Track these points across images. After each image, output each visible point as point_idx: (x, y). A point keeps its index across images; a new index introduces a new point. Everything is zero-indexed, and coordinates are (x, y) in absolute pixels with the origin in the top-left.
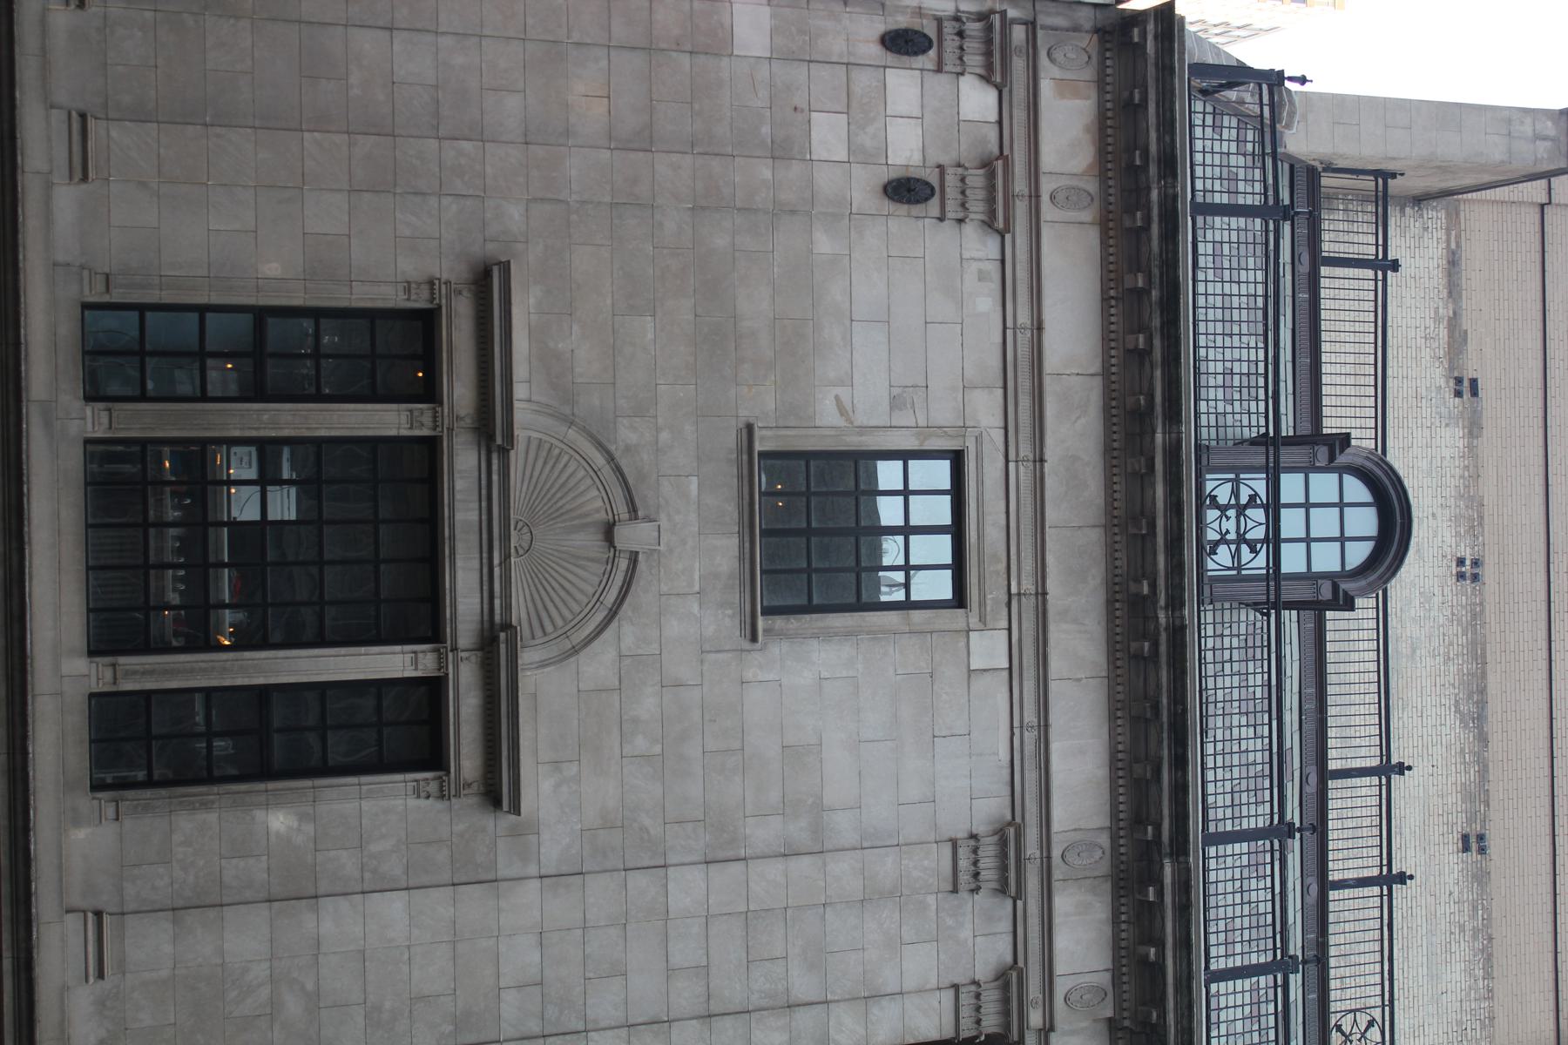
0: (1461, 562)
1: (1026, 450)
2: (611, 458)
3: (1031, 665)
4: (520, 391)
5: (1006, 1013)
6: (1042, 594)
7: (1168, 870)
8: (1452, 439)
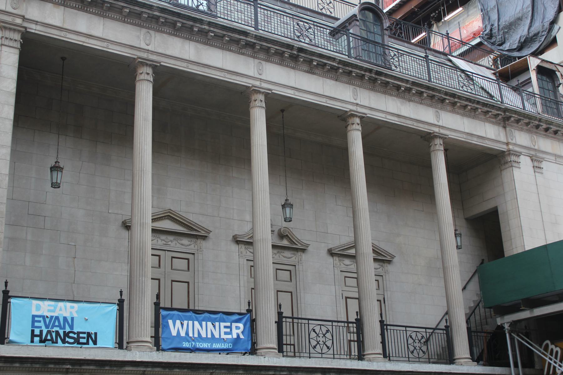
5: (14, 30)
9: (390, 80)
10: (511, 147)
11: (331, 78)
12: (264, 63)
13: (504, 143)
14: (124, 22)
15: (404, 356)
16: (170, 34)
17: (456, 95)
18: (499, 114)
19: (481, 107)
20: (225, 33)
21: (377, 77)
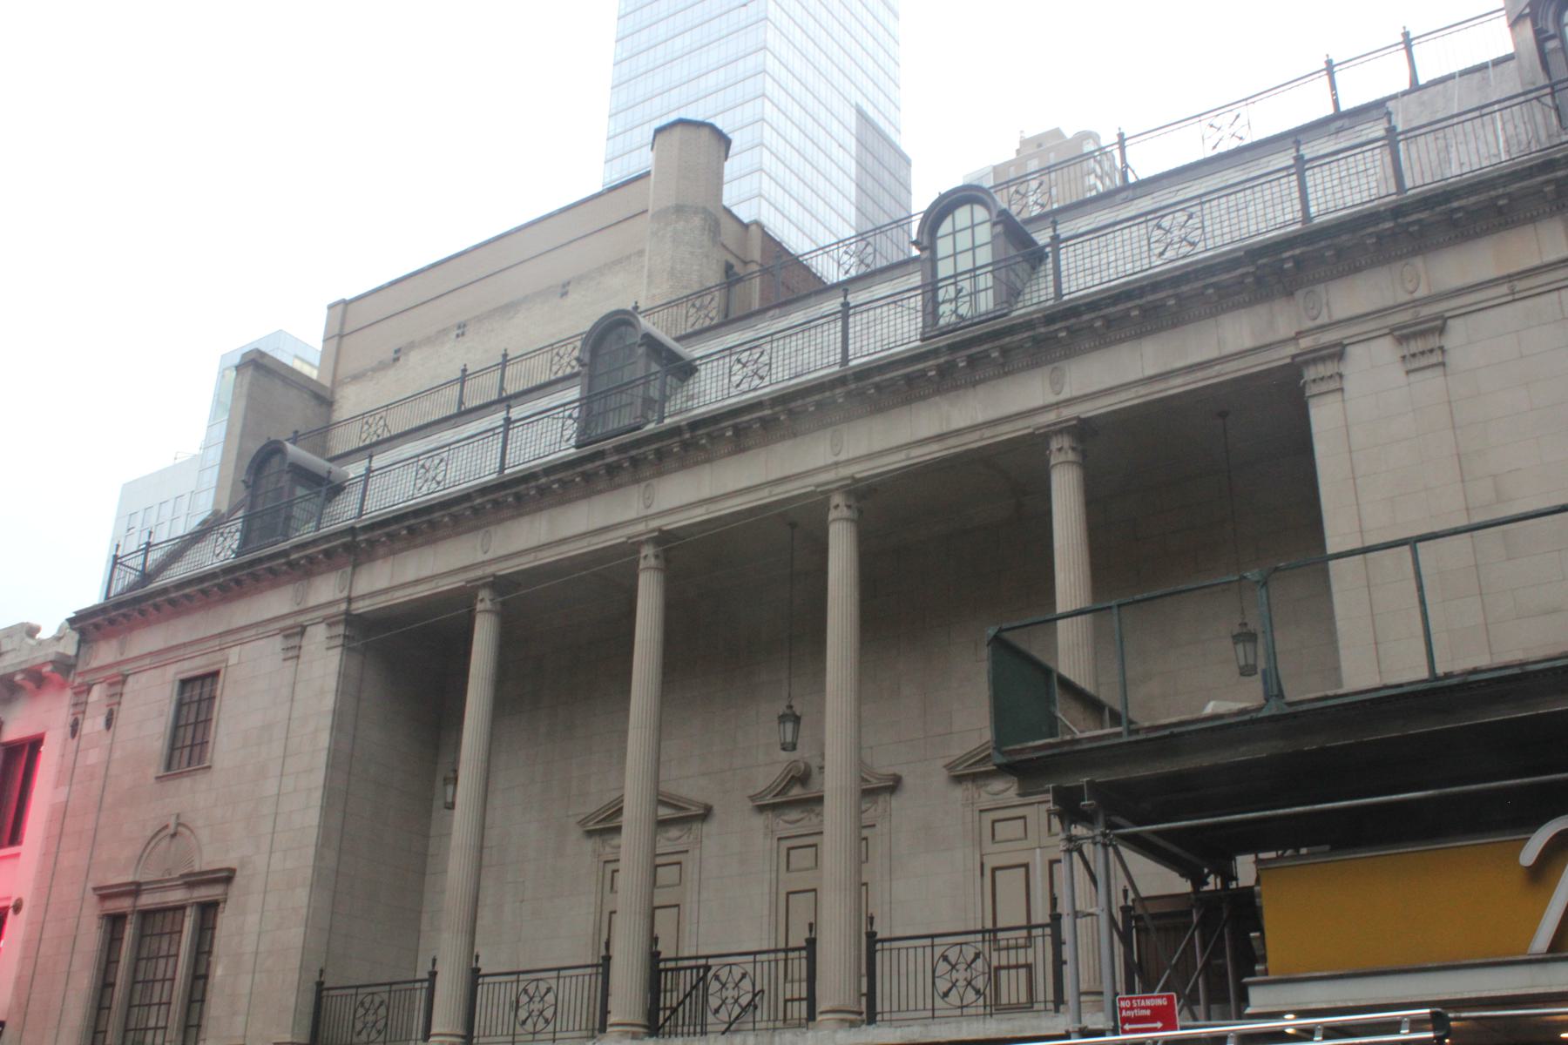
1: (181, 652)
2: (153, 838)
3: (235, 635)
4: (130, 879)
6: (220, 635)
7: (293, 557)
10: (1306, 343)
11: (783, 438)
12: (654, 482)
13: (1284, 342)
14: (459, 534)
15: (920, 1006)
16: (512, 518)
17: (1079, 306)
18: (1244, 275)
19: (1171, 292)
20: (571, 472)
21: (860, 384)
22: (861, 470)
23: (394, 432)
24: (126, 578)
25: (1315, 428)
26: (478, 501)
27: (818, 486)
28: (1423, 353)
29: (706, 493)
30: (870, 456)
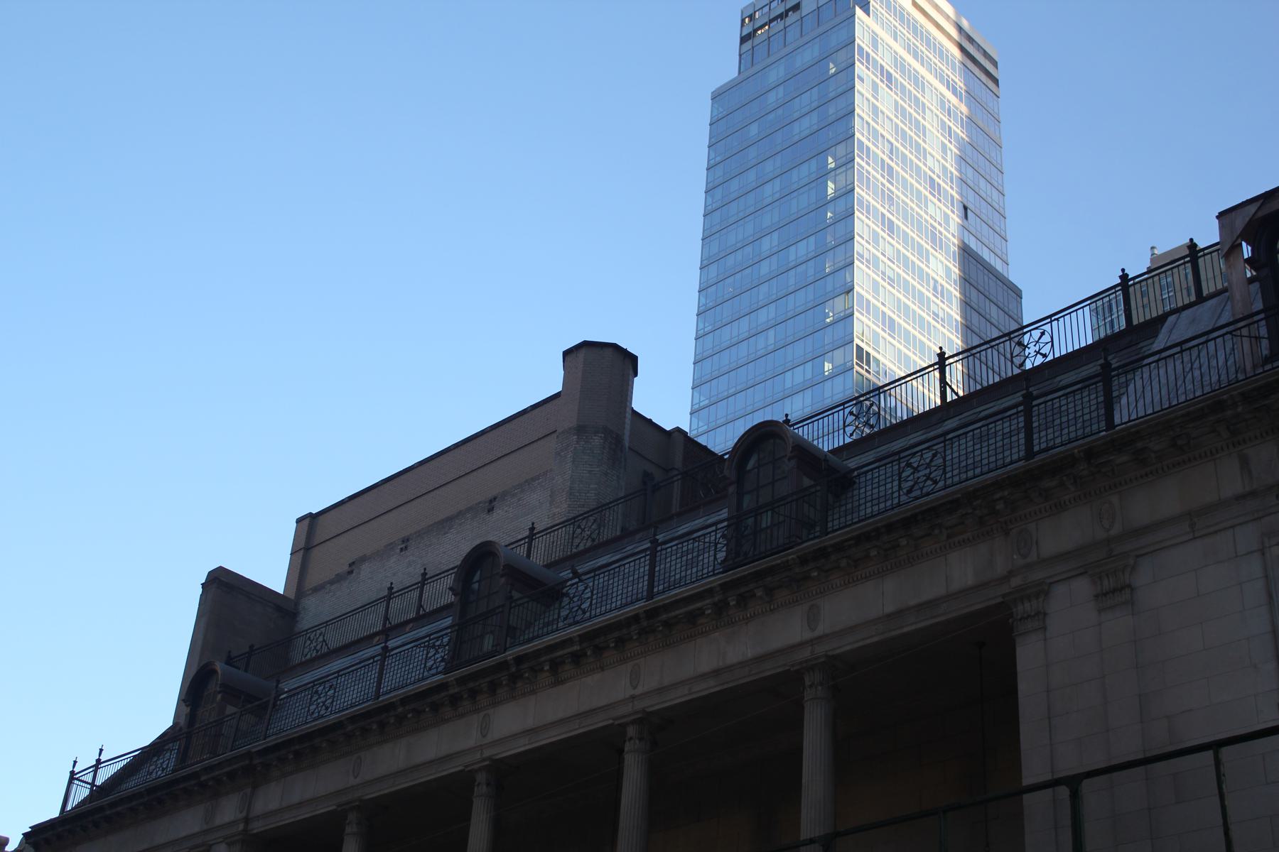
0: (402, 550)
7: (203, 778)
8: (365, 569)
9: (677, 612)
10: (1016, 582)
22: (654, 704)
23: (333, 645)
24: (80, 793)
25: (1019, 668)
26: (350, 728)
27: (615, 719)
28: (1114, 591)
29: (530, 723)
30: (661, 690)
